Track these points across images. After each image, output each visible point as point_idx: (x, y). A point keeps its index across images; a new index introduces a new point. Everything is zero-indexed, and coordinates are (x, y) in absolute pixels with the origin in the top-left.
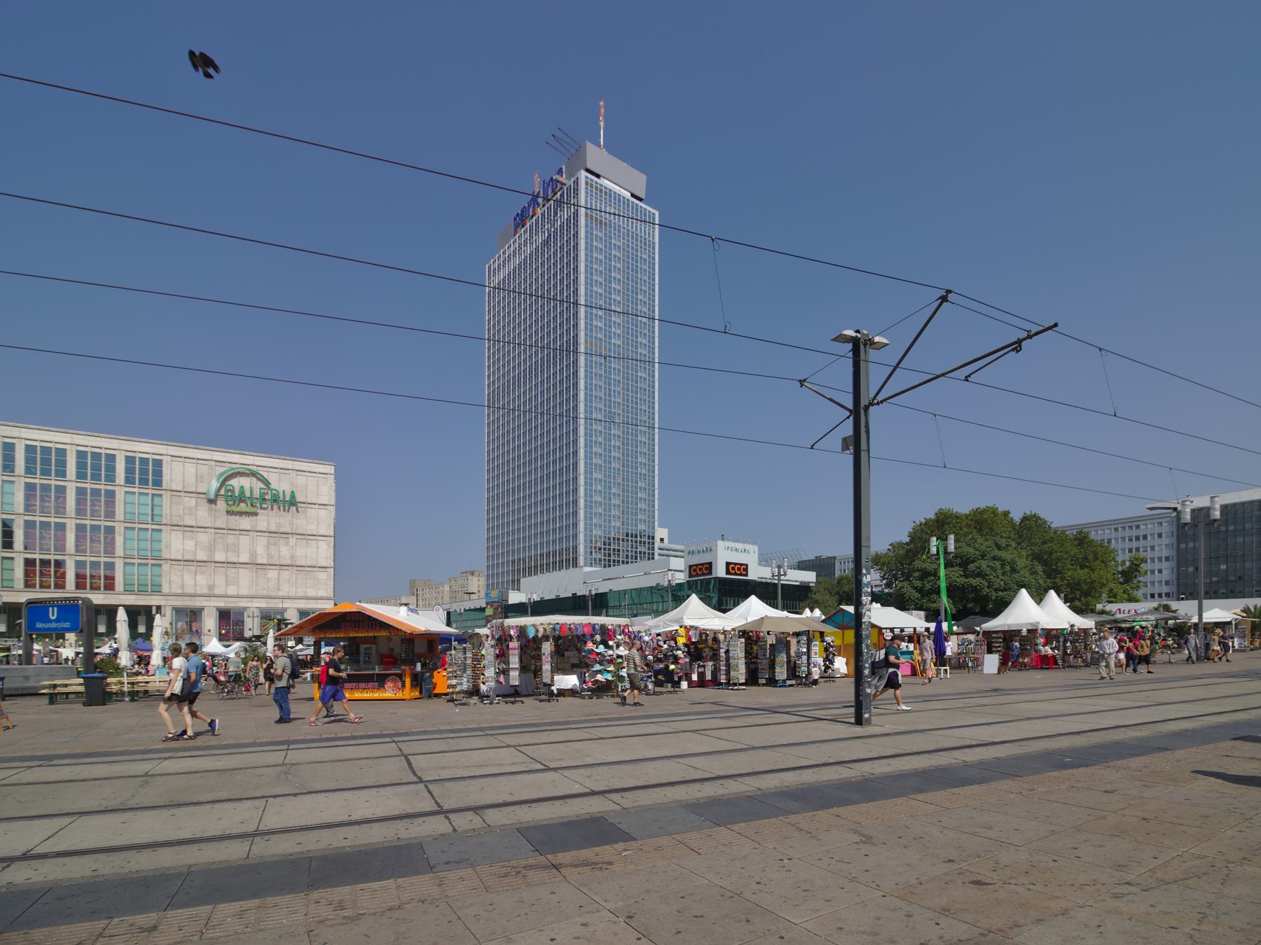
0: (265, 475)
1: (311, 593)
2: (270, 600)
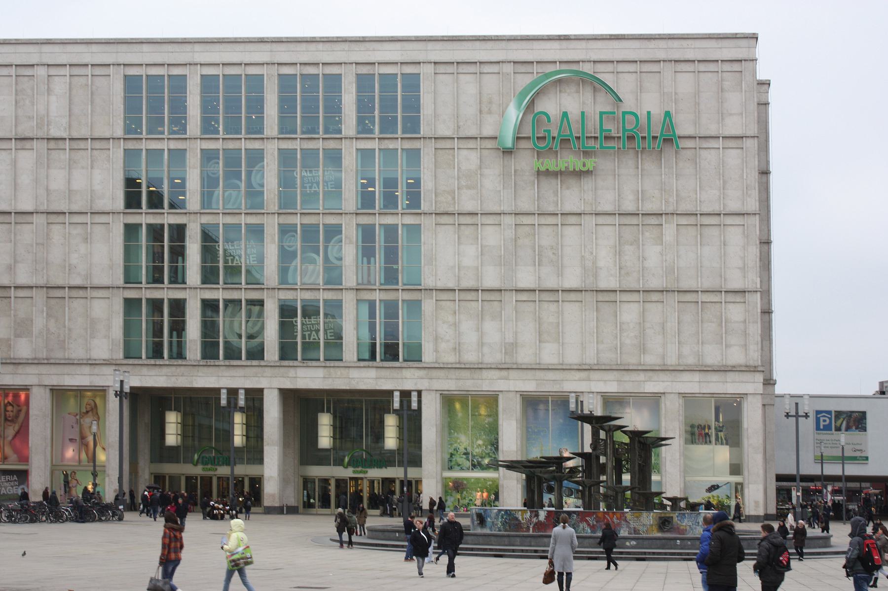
0: (608, 79)
1: (712, 356)
2: (627, 377)
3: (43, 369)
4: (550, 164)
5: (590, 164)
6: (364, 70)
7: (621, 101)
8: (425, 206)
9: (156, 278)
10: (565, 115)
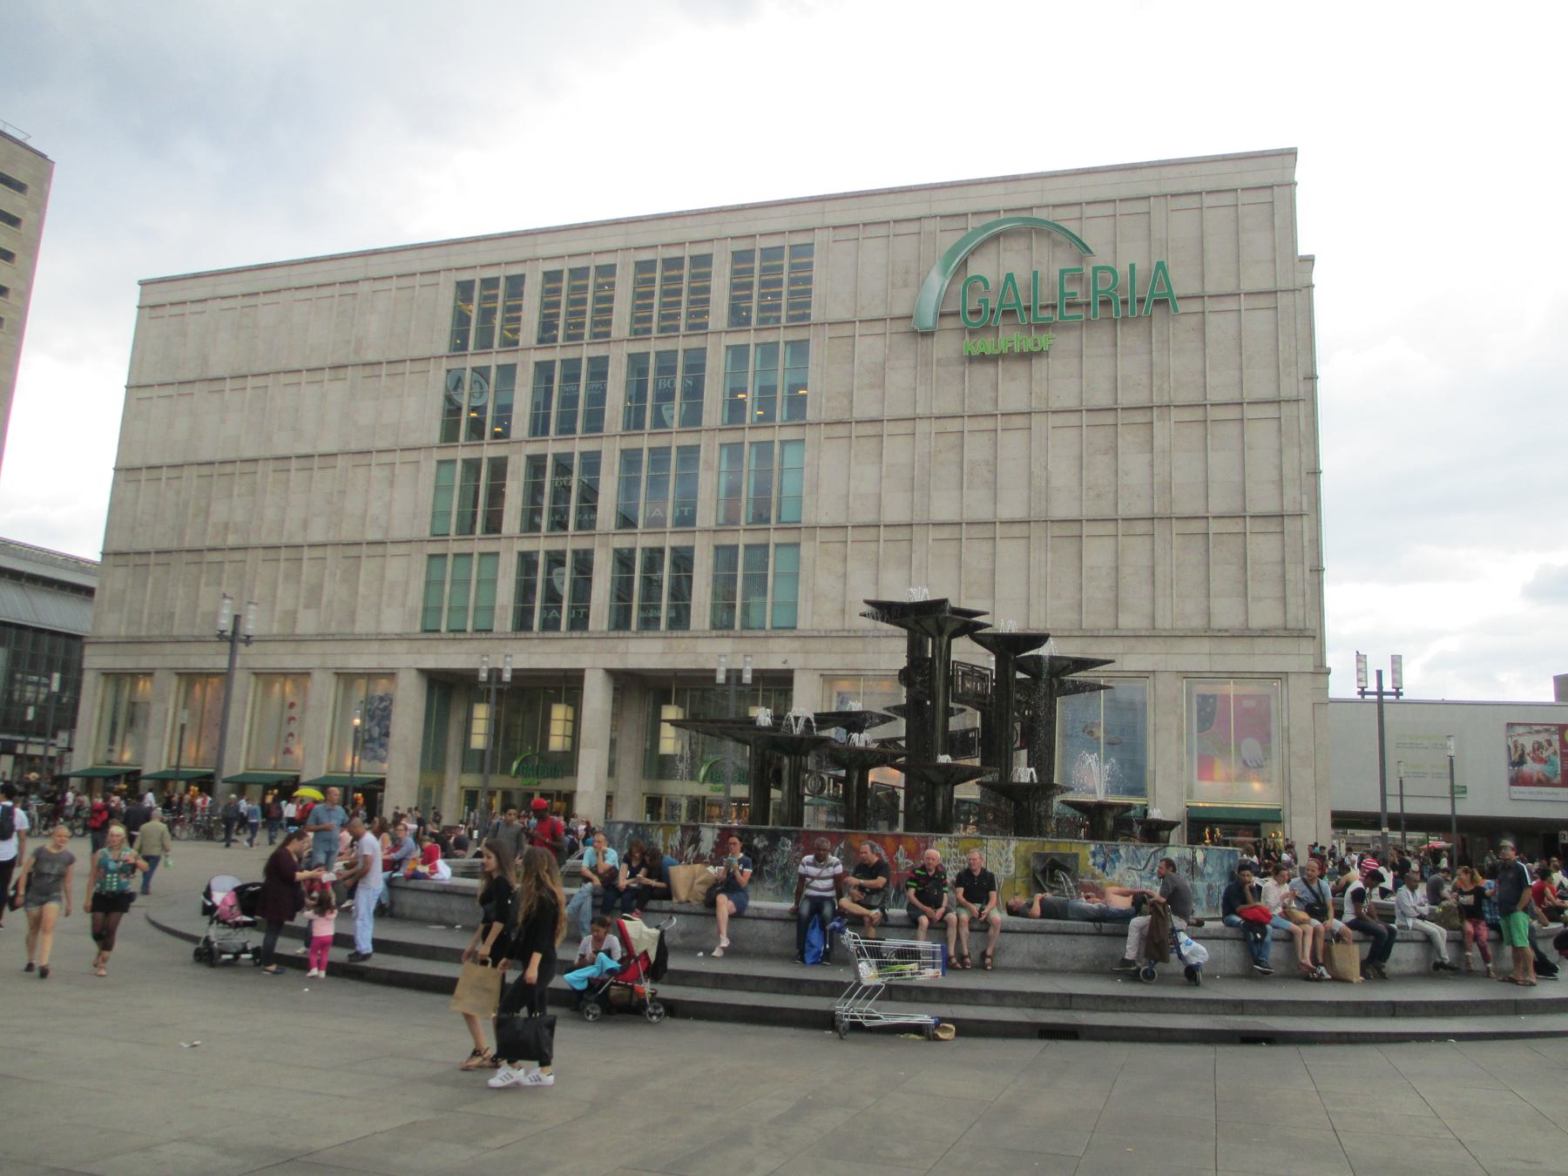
0: (1073, 227)
3: (328, 647)
4: (986, 344)
5: (1044, 340)
6: (742, 245)
7: (1090, 252)
8: (811, 415)
9: (466, 528)
10: (1010, 277)
